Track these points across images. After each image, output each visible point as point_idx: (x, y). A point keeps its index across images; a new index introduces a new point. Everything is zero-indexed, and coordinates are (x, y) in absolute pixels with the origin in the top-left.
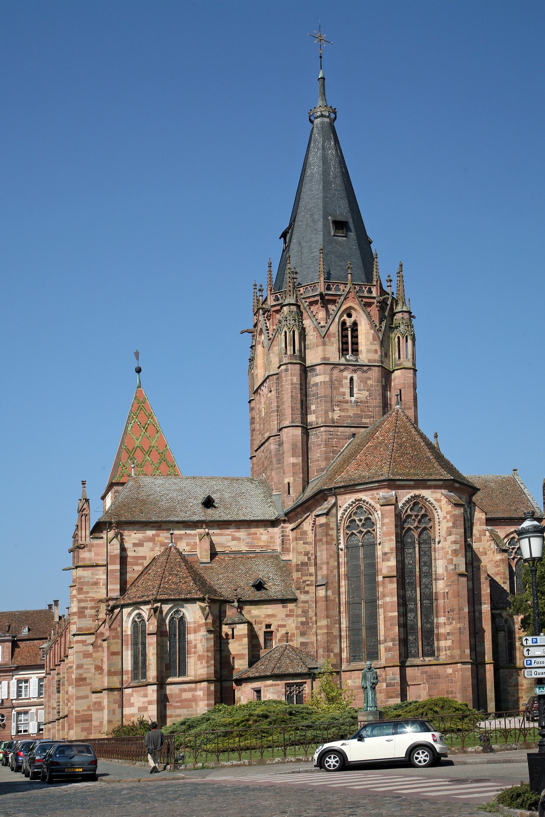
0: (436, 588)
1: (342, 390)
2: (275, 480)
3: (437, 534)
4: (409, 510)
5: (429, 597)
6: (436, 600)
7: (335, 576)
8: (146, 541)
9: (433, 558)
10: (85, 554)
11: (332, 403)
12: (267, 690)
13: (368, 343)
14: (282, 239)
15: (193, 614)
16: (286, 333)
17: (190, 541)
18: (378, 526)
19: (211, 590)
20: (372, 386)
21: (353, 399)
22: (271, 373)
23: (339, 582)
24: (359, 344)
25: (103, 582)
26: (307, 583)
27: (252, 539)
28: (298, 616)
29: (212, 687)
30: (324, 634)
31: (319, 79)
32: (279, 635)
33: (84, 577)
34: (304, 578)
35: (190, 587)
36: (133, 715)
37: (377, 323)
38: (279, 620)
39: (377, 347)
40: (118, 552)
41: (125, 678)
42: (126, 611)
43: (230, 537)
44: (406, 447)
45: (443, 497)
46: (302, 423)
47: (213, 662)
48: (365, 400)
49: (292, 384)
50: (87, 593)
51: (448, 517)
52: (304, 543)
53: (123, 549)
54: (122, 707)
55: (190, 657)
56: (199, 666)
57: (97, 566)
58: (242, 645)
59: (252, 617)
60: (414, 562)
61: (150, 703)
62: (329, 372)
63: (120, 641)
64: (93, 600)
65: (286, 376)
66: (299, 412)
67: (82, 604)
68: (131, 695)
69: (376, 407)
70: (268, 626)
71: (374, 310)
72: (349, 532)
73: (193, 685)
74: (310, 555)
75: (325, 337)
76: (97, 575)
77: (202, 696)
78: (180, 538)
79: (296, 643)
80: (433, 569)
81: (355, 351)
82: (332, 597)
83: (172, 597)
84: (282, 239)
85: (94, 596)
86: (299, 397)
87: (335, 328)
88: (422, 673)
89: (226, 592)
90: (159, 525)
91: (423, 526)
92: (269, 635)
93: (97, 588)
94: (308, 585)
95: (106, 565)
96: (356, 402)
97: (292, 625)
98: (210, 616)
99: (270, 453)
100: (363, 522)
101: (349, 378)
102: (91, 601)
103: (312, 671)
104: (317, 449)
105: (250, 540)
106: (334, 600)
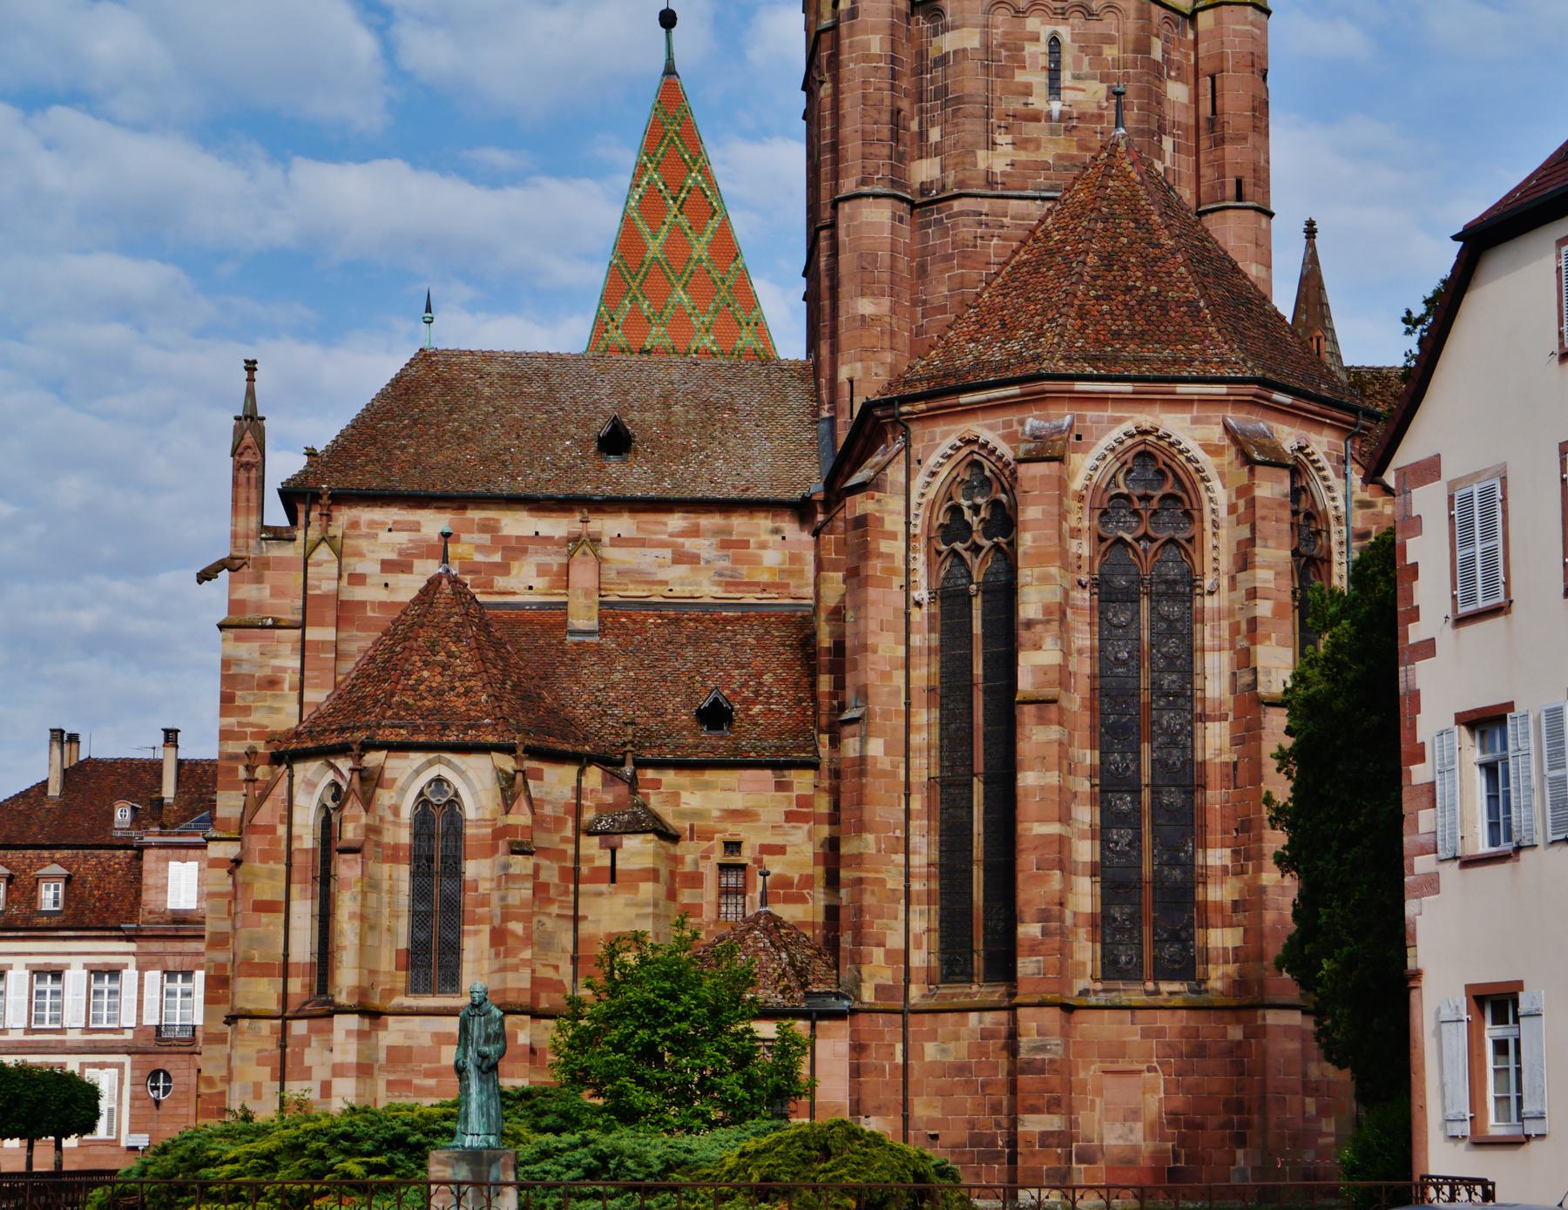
1: (1021, 77)
8: (420, 556)
9: (1198, 643)
25: (290, 679)
46: (893, 183)
50: (246, 710)
60: (1135, 655)
62: (981, 19)
65: (851, 35)
66: (886, 151)
68: (305, 1042)
76: (275, 657)
80: (1198, 682)
82: (885, 763)
85: (265, 722)
86: (887, 102)
93: (276, 697)
101: (1044, 38)
102: (255, 736)
106: (894, 775)
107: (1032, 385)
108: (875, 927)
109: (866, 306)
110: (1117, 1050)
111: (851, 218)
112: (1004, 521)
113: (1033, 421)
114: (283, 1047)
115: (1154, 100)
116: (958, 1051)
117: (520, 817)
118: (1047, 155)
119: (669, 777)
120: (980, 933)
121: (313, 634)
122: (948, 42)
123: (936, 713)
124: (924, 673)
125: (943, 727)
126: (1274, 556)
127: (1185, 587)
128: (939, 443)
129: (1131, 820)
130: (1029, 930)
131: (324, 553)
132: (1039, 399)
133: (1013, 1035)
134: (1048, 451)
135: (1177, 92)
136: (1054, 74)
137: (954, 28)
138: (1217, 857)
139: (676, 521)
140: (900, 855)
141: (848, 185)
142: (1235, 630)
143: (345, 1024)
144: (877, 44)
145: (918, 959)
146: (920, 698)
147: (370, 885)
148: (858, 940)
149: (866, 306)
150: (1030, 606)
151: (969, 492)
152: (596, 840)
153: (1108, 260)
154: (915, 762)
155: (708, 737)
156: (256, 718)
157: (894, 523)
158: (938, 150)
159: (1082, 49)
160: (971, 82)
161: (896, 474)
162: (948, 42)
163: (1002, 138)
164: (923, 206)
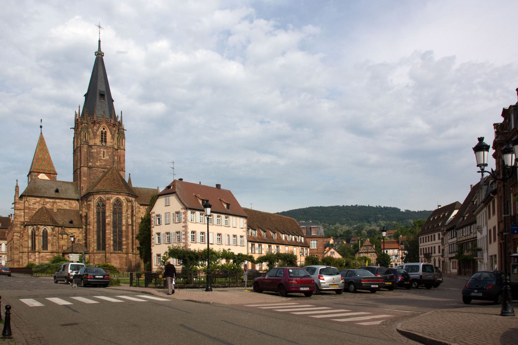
10: (17, 206)
25: (23, 216)
41: (29, 249)
42: (29, 227)
78: (47, 202)
81: (106, 142)
107: (107, 193)
108: (91, 245)
109: (84, 179)
110: (115, 257)
112: (104, 205)
113: (107, 196)
115: (114, 158)
116: (99, 257)
117: (54, 233)
118: (103, 164)
119: (67, 229)
120: (102, 245)
121: (26, 211)
122: (93, 151)
124: (95, 220)
126: (130, 211)
127: (121, 213)
128: (97, 197)
129: (116, 235)
130: (107, 246)
131: (27, 202)
132: (108, 194)
133: (106, 255)
134: (109, 199)
135: (116, 158)
138: (124, 239)
139: (64, 201)
140: (93, 238)
141: (82, 165)
143: (37, 253)
144: (85, 150)
145: (95, 248)
147: (39, 239)
148: (89, 246)
149: (84, 179)
150: (107, 214)
151: (100, 202)
153: (114, 180)
155: (71, 224)
157: (93, 205)
158: (92, 162)
160: (95, 155)
161: (93, 200)
162: (93, 151)
164: (90, 168)
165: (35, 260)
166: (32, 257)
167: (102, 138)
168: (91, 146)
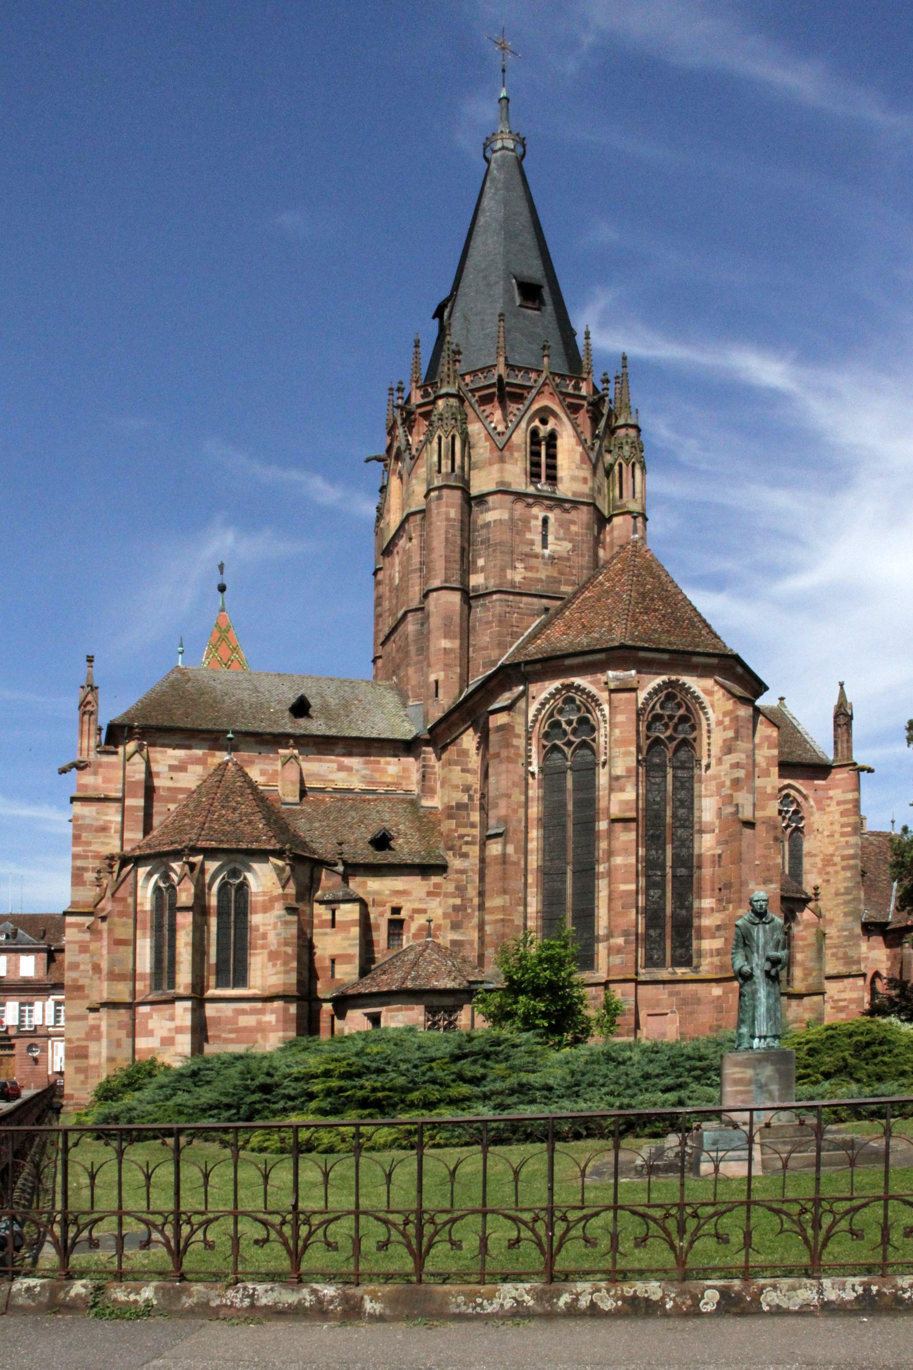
0: (700, 848)
1: (529, 536)
2: (413, 682)
3: (705, 753)
4: (658, 706)
5: (687, 862)
6: (700, 867)
7: (520, 821)
8: (192, 763)
9: (696, 794)
11: (515, 554)
12: (392, 1017)
13: (574, 466)
14: (437, 320)
15: (262, 879)
16: (440, 438)
17: (266, 767)
18: (602, 731)
19: (295, 839)
20: (576, 534)
21: (547, 552)
22: (413, 509)
23: (527, 833)
24: (559, 468)
26: (466, 839)
27: (373, 770)
28: (447, 895)
29: (293, 1009)
30: (496, 921)
31: (500, 100)
32: (413, 927)
33: (83, 817)
34: (462, 831)
35: (260, 834)
36: (151, 1050)
37: (587, 435)
38: (414, 900)
39: (586, 473)
40: (141, 776)
41: (139, 986)
43: (335, 766)
44: (652, 599)
45: (716, 688)
46: (462, 583)
47: (294, 964)
48: (565, 555)
49: (448, 519)
50: (88, 843)
51: (727, 721)
52: (463, 771)
53: (149, 774)
54: (133, 1035)
55: (255, 954)
56: (270, 970)
57: (107, 799)
58: (348, 939)
59: (368, 893)
60: (664, 799)
61: (179, 1030)
62: (509, 505)
63: (131, 921)
64: (97, 856)
65: (438, 506)
66: (458, 567)
67: (79, 863)
68: (149, 1016)
69: (582, 567)
70: (396, 910)
71: (583, 417)
72: (549, 744)
73: (259, 1005)
74: (471, 792)
75: (502, 449)
76: (106, 815)
77: (274, 1023)
79: (447, 937)
80: (696, 813)
81: (552, 479)
82: (514, 858)
83: (225, 846)
84: (437, 320)
85: (100, 850)
86: (459, 542)
87: (520, 437)
88: (671, 994)
89: (323, 847)
90: (214, 739)
91: (682, 736)
92: (396, 926)
94: (467, 843)
95: (121, 800)
96: (552, 558)
97: (437, 909)
98: (291, 884)
99: (406, 639)
100: (574, 724)
101: (541, 518)
102: (95, 857)
103: (474, 987)
104: (486, 629)
105: (368, 772)
106: (518, 864)
111: (437, 599)
114: (134, 1020)
123: (541, 832)
125: (545, 838)
136: (545, 538)
137: (494, 509)
142: (721, 785)
144: (454, 513)
146: (533, 823)
152: (323, 907)
154: (529, 858)
156: (93, 848)
158: (483, 569)
159: (560, 525)
162: (490, 516)
163: (519, 565)
165: (168, 1042)
166: (151, 1025)
167: (536, 464)
168: (481, 499)
